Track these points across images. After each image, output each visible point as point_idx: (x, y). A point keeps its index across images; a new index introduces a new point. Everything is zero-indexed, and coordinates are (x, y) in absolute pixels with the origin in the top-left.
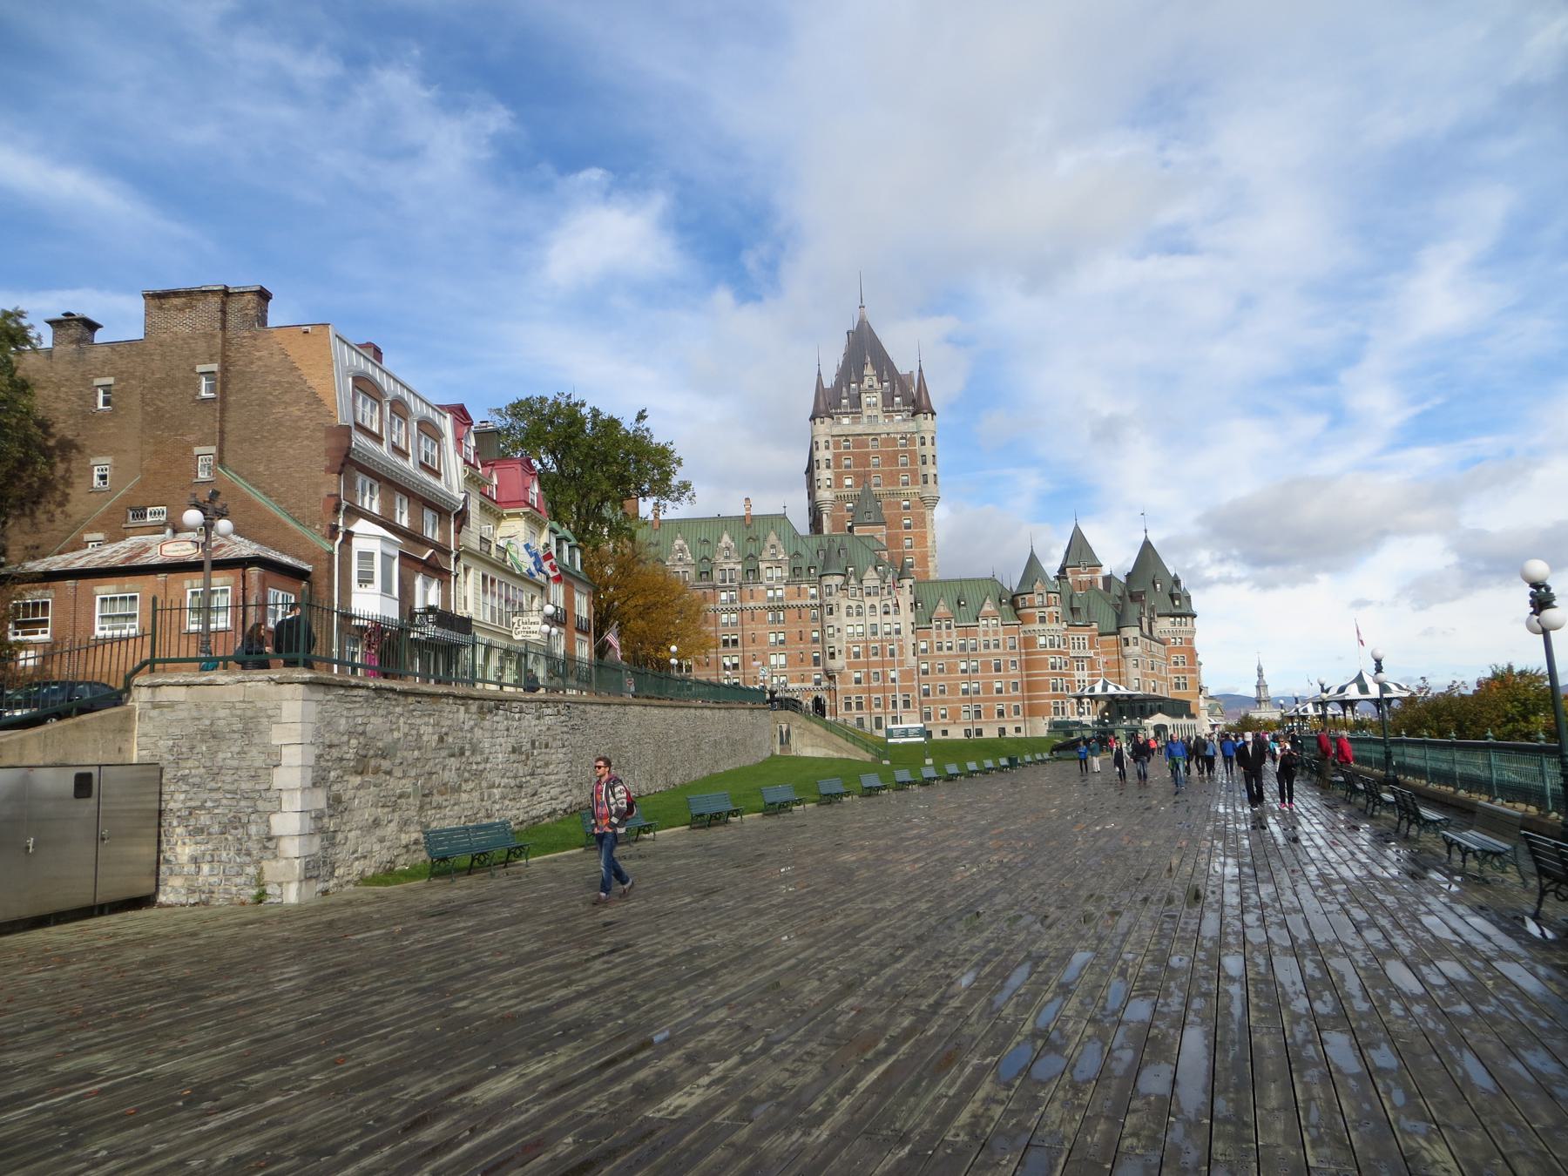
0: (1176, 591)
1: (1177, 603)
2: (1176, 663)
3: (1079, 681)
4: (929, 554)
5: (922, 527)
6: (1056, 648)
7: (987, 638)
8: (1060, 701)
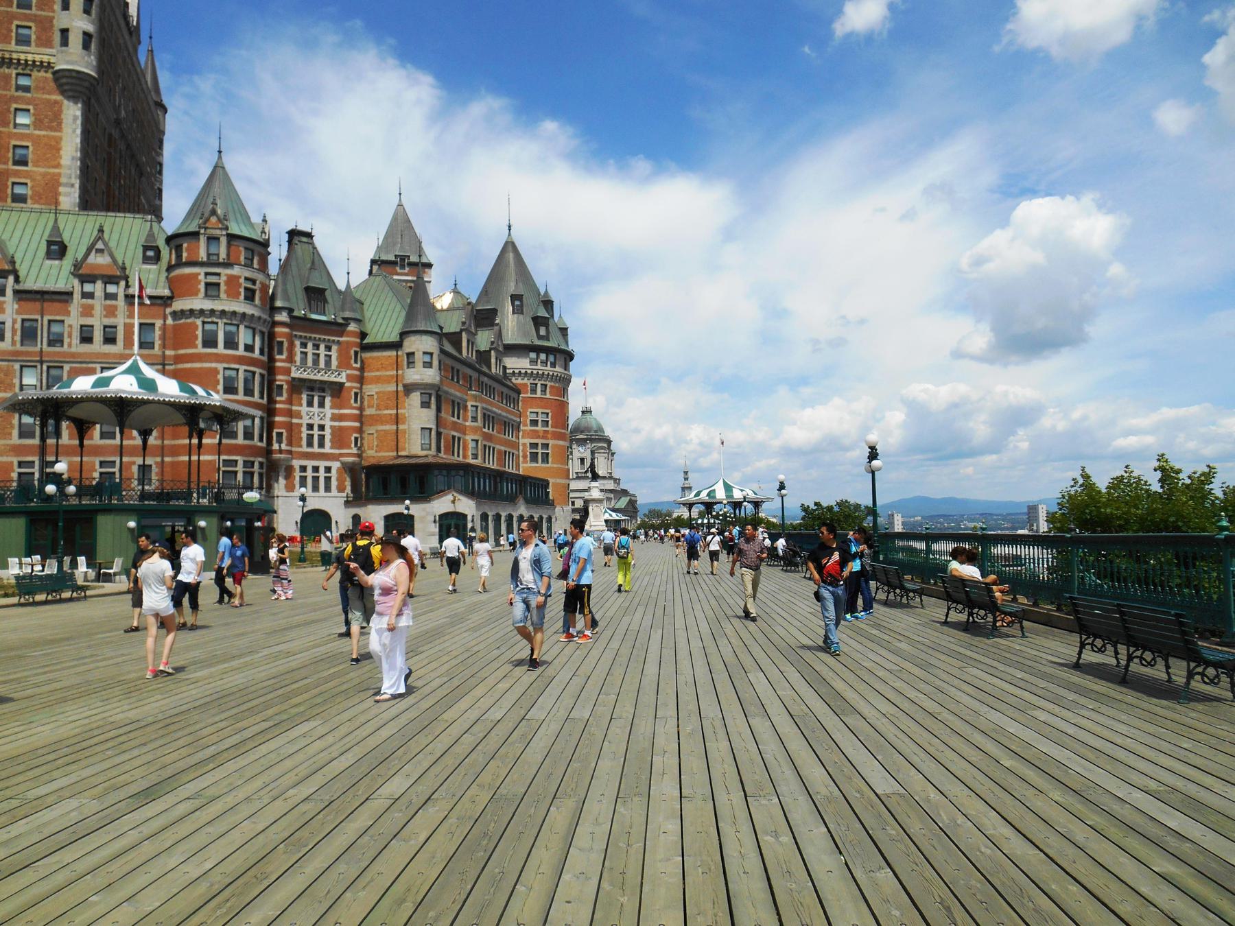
0: (542, 313)
1: (543, 331)
2: (534, 423)
3: (310, 427)
4: (63, 180)
5: (51, 129)
6: (241, 351)
7: (88, 321)
8: (240, 459)
